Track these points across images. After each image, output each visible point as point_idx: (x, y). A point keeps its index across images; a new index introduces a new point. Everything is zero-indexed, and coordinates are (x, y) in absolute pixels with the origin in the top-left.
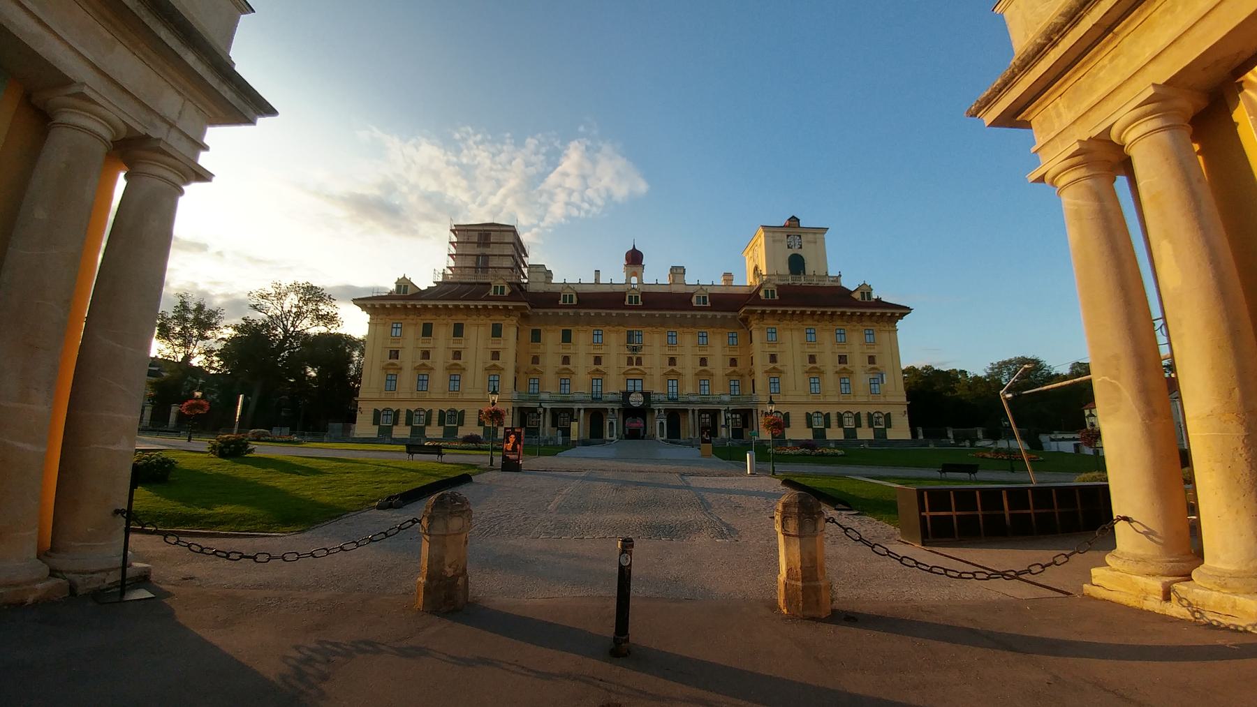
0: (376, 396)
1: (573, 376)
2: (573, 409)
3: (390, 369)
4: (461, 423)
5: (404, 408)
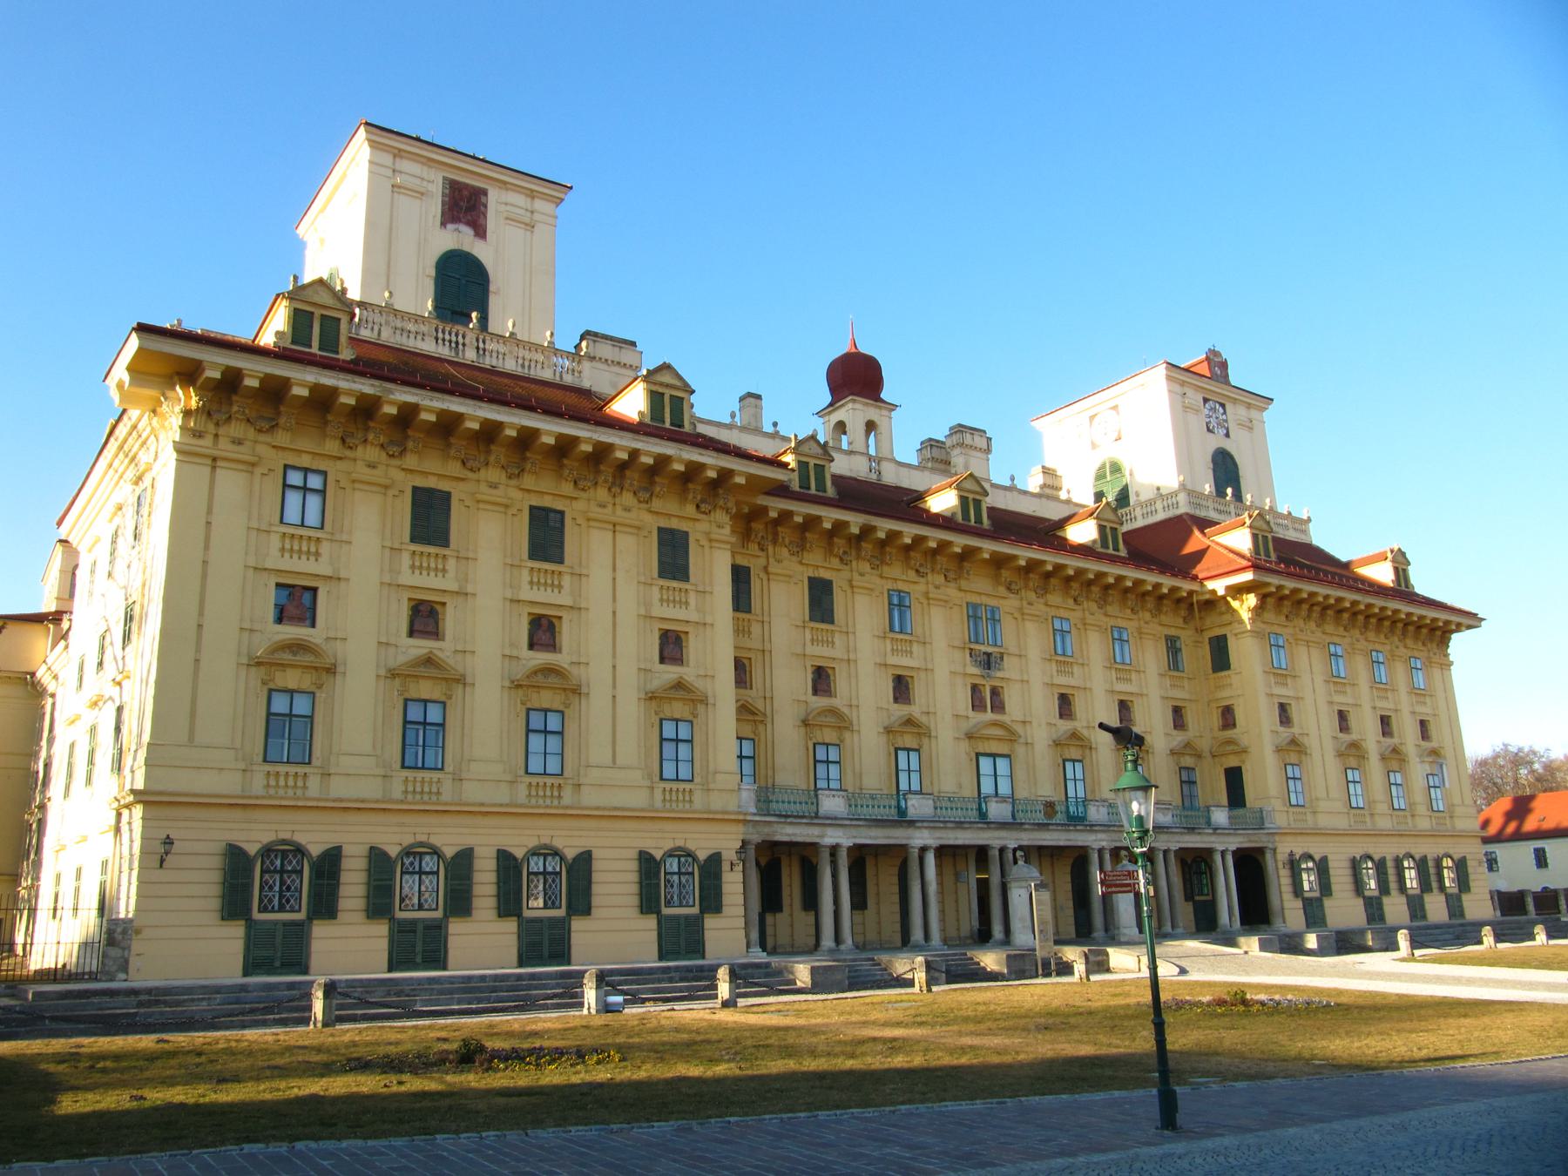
0: (226, 783)
1: (847, 735)
2: (903, 849)
3: (283, 666)
4: (581, 902)
5: (486, 842)
